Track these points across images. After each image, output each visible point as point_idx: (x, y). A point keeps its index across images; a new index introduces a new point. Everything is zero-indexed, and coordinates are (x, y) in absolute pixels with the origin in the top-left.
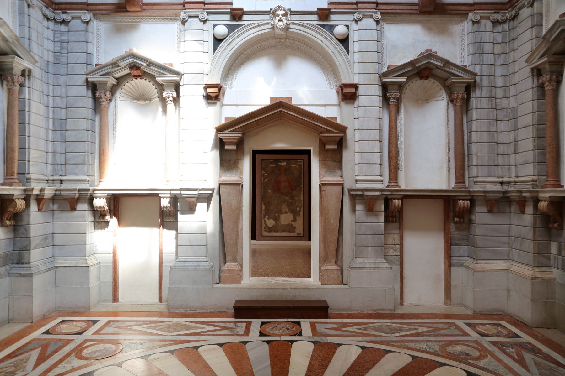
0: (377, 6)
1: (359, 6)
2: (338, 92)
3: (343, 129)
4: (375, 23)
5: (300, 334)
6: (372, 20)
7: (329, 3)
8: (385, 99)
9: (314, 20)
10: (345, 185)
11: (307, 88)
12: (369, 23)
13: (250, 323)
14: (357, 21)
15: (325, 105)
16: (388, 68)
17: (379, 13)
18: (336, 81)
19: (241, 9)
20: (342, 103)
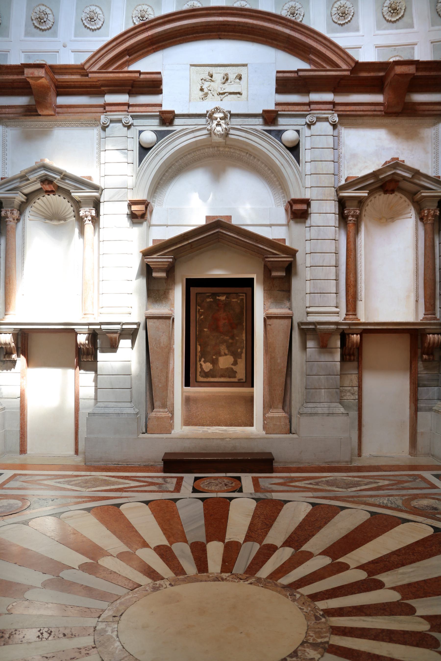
0: (334, 107)
1: (312, 106)
2: (286, 210)
3: (292, 253)
4: (332, 127)
5: (241, 490)
6: (327, 124)
7: (277, 104)
8: (343, 218)
9: (258, 124)
10: (294, 318)
11: (251, 205)
12: (324, 127)
13: (182, 478)
14: (309, 125)
15: (271, 226)
16: (346, 180)
17: (336, 115)
18: (284, 197)
19: (172, 112)
20: (292, 222)
